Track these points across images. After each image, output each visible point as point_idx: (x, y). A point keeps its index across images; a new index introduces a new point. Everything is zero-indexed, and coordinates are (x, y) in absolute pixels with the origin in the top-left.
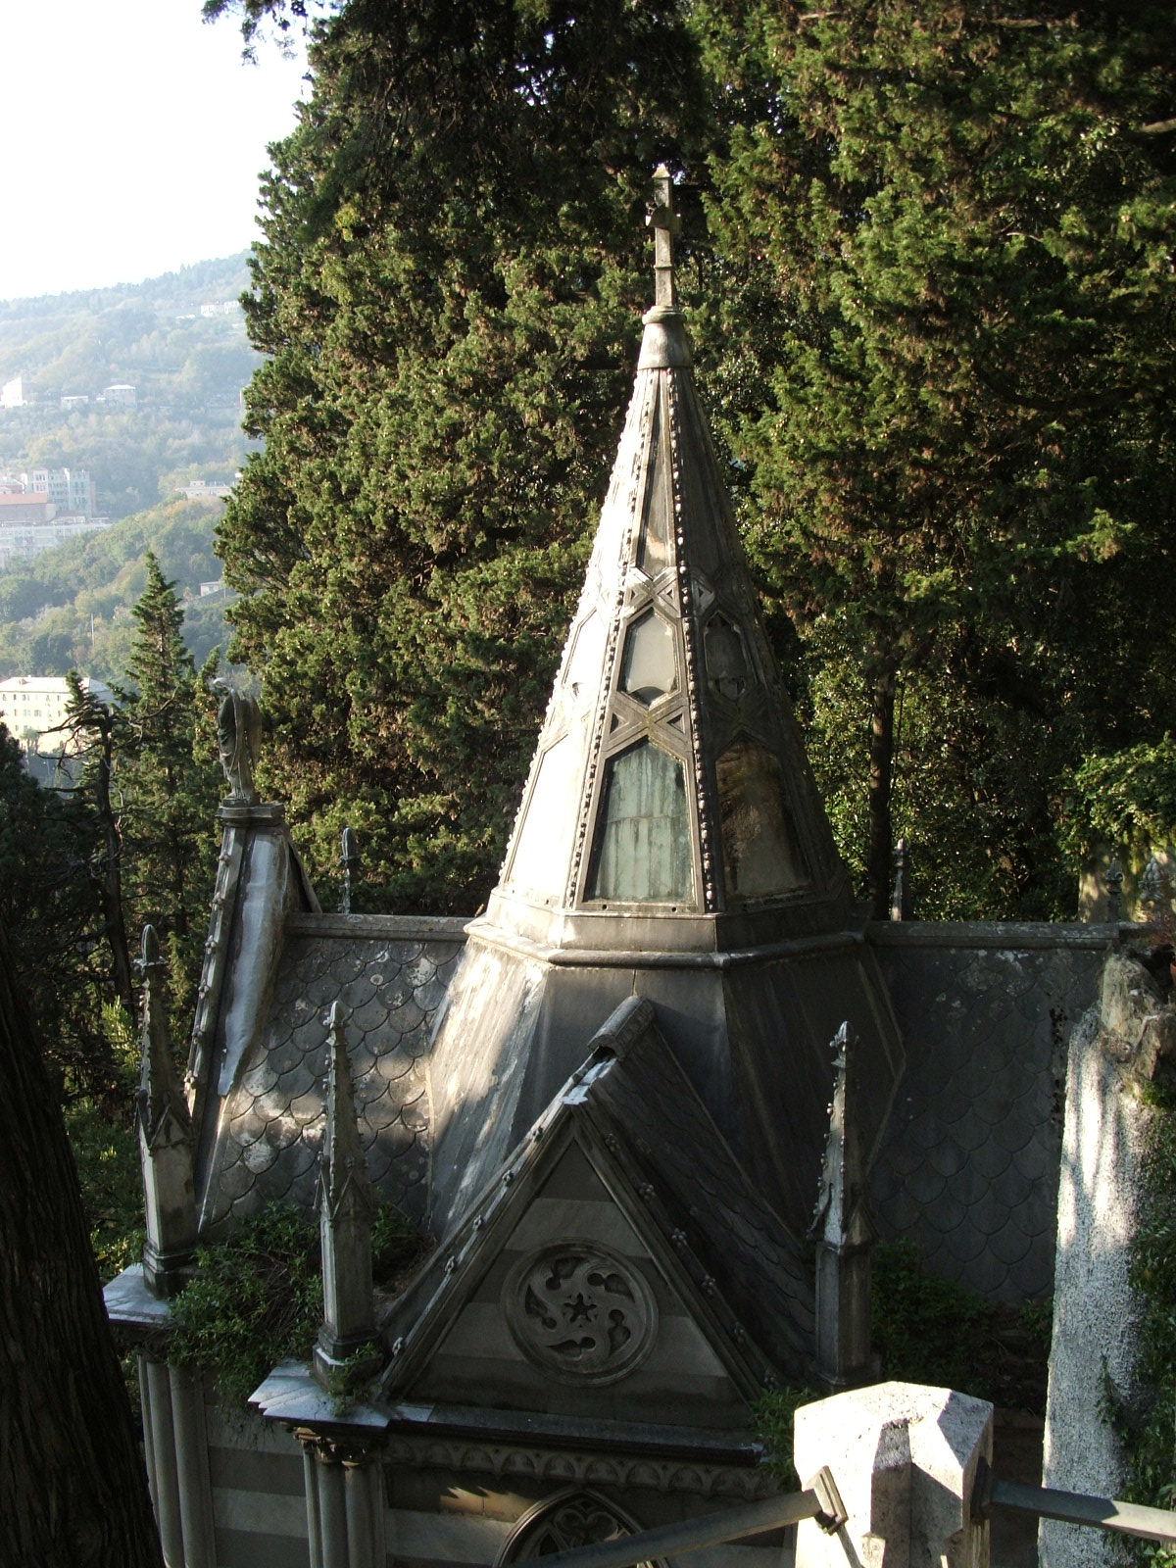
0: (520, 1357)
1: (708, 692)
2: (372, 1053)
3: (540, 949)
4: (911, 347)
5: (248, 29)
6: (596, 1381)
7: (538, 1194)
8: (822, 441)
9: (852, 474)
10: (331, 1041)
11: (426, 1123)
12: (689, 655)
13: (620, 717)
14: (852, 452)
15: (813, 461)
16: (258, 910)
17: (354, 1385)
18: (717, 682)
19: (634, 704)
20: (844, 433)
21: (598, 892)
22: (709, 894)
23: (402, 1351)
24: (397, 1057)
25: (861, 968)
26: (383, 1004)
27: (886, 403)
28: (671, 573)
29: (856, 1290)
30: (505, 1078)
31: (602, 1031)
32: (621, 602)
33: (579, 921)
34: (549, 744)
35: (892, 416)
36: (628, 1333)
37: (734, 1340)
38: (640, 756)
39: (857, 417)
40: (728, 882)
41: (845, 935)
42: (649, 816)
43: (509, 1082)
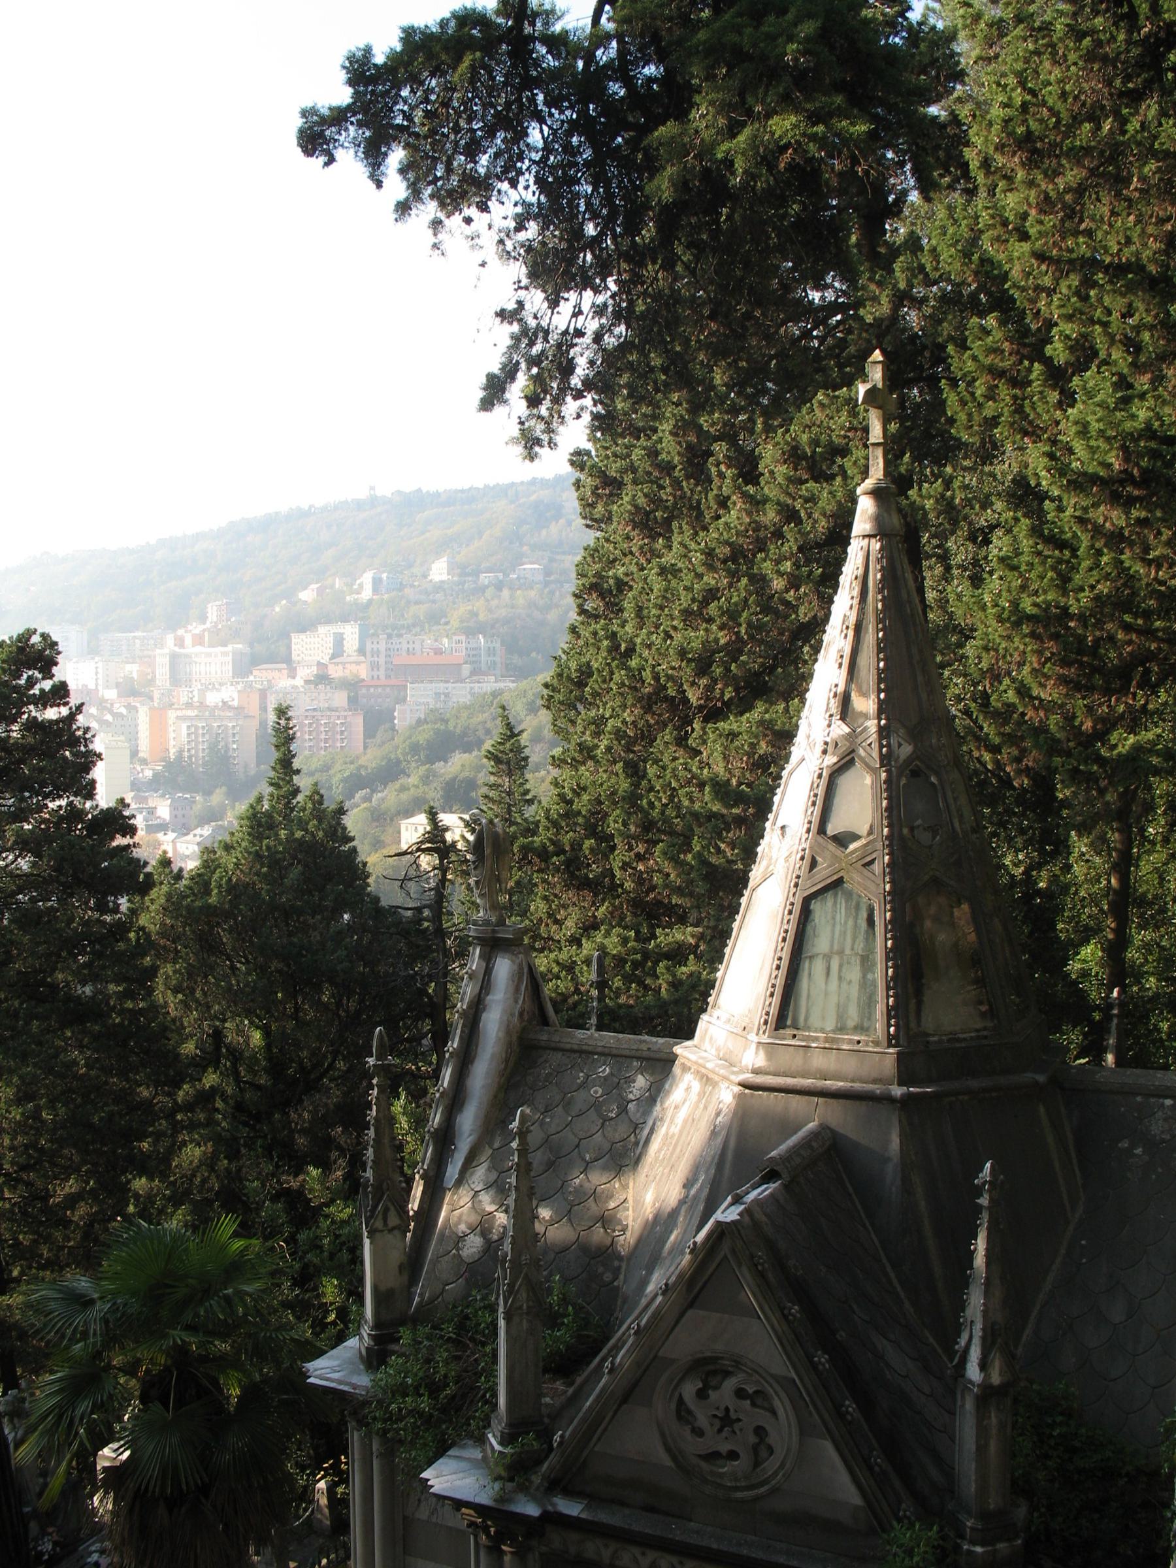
0: (668, 1462)
1: (902, 838)
2: (584, 1159)
3: (733, 1073)
4: (1113, 517)
5: (436, 224)
6: (739, 1495)
7: (691, 1305)
8: (1027, 605)
9: (1056, 637)
10: (514, 1145)
11: (624, 1230)
12: (885, 803)
13: (819, 859)
14: (1055, 615)
15: (1017, 624)
16: (493, 1022)
17: (515, 1472)
18: (912, 829)
19: (832, 846)
20: (1049, 598)
21: (789, 1022)
22: (892, 1029)
23: (561, 1444)
24: (605, 1168)
25: (1042, 1109)
26: (600, 1115)
27: (1091, 569)
28: (872, 725)
29: (994, 1431)
30: (693, 1192)
31: (773, 1154)
32: (825, 752)
33: (770, 1049)
34: (757, 881)
35: (1098, 582)
36: (771, 1450)
37: (870, 1468)
38: (836, 895)
39: (1064, 581)
40: (912, 1017)
41: (1028, 1076)
42: (841, 952)
43: (695, 1197)
